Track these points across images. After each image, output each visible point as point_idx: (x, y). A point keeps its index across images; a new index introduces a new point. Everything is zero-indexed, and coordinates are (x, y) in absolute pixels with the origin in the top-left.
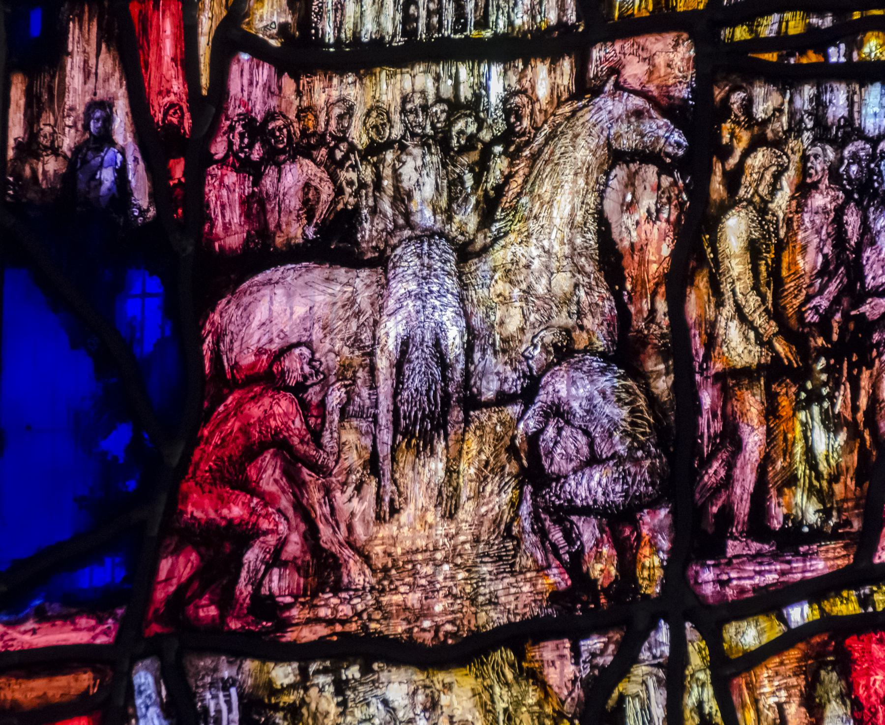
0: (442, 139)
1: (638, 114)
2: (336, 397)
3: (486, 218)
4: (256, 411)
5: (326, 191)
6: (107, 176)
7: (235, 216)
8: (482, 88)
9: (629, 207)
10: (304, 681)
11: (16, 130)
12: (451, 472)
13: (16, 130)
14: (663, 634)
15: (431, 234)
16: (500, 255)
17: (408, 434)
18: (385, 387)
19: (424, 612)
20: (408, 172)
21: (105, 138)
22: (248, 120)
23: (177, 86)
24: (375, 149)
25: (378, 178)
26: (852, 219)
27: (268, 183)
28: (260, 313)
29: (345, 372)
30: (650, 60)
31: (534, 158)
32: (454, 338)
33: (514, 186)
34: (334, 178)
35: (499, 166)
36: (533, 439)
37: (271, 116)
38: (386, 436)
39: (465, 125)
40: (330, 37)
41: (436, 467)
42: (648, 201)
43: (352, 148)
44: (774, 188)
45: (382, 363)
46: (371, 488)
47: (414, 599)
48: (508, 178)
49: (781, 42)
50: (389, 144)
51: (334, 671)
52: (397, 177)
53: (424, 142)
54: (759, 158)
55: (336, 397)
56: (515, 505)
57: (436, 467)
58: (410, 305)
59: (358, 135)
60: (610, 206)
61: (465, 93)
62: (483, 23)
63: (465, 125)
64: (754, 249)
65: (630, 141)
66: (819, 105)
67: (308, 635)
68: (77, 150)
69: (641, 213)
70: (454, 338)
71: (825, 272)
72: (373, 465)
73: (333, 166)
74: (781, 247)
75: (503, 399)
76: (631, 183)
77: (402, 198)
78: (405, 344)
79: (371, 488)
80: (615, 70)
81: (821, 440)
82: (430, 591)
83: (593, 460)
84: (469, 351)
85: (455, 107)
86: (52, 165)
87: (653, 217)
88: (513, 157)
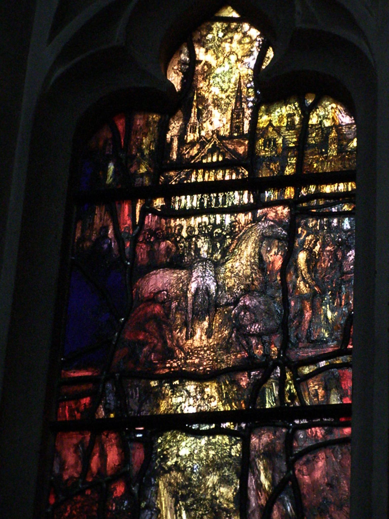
0: (210, 235)
1: (272, 226)
2: (174, 305)
3: (224, 254)
4: (149, 310)
5: (174, 249)
6: (106, 246)
7: (145, 256)
8: (223, 221)
9: (269, 252)
10: (161, 385)
11: (78, 235)
12: (210, 324)
13: (78, 235)
14: (278, 370)
15: (205, 260)
16: (229, 265)
17: (197, 315)
18: (190, 301)
19: (200, 364)
20: (199, 244)
21: (106, 236)
22: (150, 230)
23: (129, 222)
24: (189, 238)
25: (190, 245)
26: (339, 254)
27: (156, 247)
28: (152, 283)
29: (177, 298)
30: (276, 212)
31: (239, 239)
32: (213, 288)
33: (233, 247)
34: (176, 246)
35: (229, 241)
36: (237, 316)
37: (157, 229)
38: (190, 316)
39: (219, 231)
40: (177, 208)
41: (206, 324)
42: (275, 250)
43: (182, 237)
44: (315, 245)
45: (189, 295)
46: (184, 331)
47: (197, 361)
48: (230, 245)
49: (318, 207)
50: (194, 236)
51: (170, 383)
52: (196, 245)
53: (205, 235)
54: (310, 238)
55: (174, 305)
56: (231, 334)
57: (206, 324)
58: (200, 279)
59: (184, 234)
60: (263, 251)
61: (218, 222)
62: (224, 203)
63: (219, 231)
64: (308, 262)
65: (269, 233)
66: (329, 224)
67: (162, 372)
68: (97, 239)
69: (272, 253)
70: (213, 288)
71: (332, 267)
72: (185, 324)
73: (176, 243)
74: (317, 261)
75: (227, 304)
76: (269, 245)
77: (197, 250)
78: (197, 289)
79: (184, 331)
80: (265, 215)
81: (329, 314)
82: (201, 359)
83: (255, 322)
84: (217, 291)
85: (215, 226)
86: (88, 244)
87: (276, 254)
88: (233, 239)
